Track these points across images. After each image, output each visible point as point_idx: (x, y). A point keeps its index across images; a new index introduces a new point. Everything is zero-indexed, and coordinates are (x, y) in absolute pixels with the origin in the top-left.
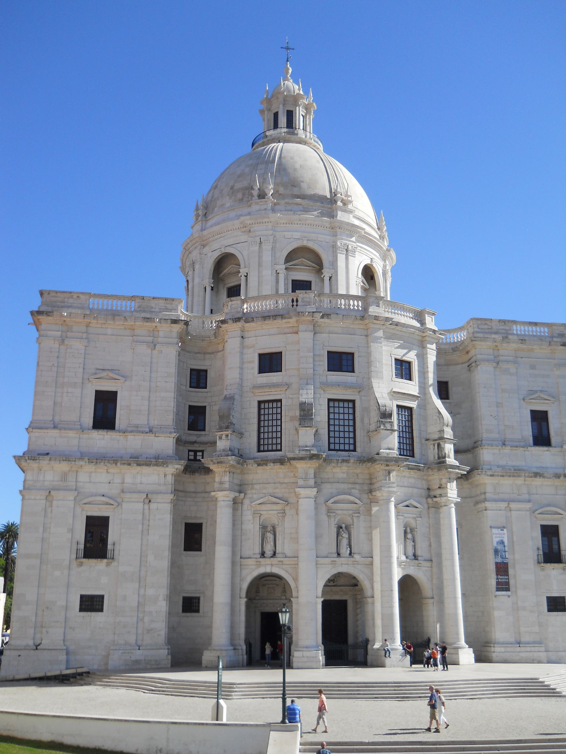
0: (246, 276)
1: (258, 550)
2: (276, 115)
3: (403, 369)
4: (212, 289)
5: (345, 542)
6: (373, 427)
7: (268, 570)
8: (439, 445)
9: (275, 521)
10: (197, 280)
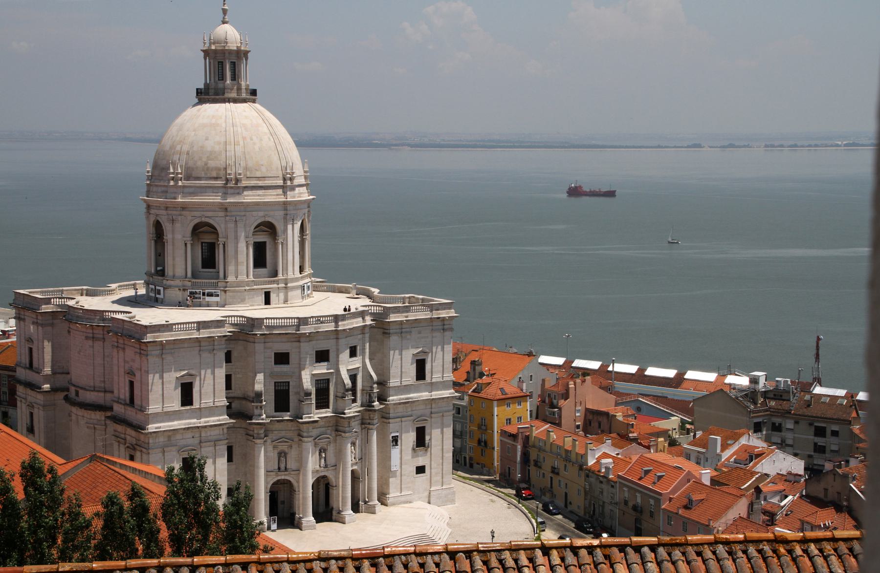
0: (224, 245)
1: (276, 467)
2: (221, 64)
3: (353, 353)
4: (192, 245)
5: (323, 461)
6: (340, 395)
7: (283, 477)
8: (370, 395)
9: (286, 450)
10: (179, 236)
